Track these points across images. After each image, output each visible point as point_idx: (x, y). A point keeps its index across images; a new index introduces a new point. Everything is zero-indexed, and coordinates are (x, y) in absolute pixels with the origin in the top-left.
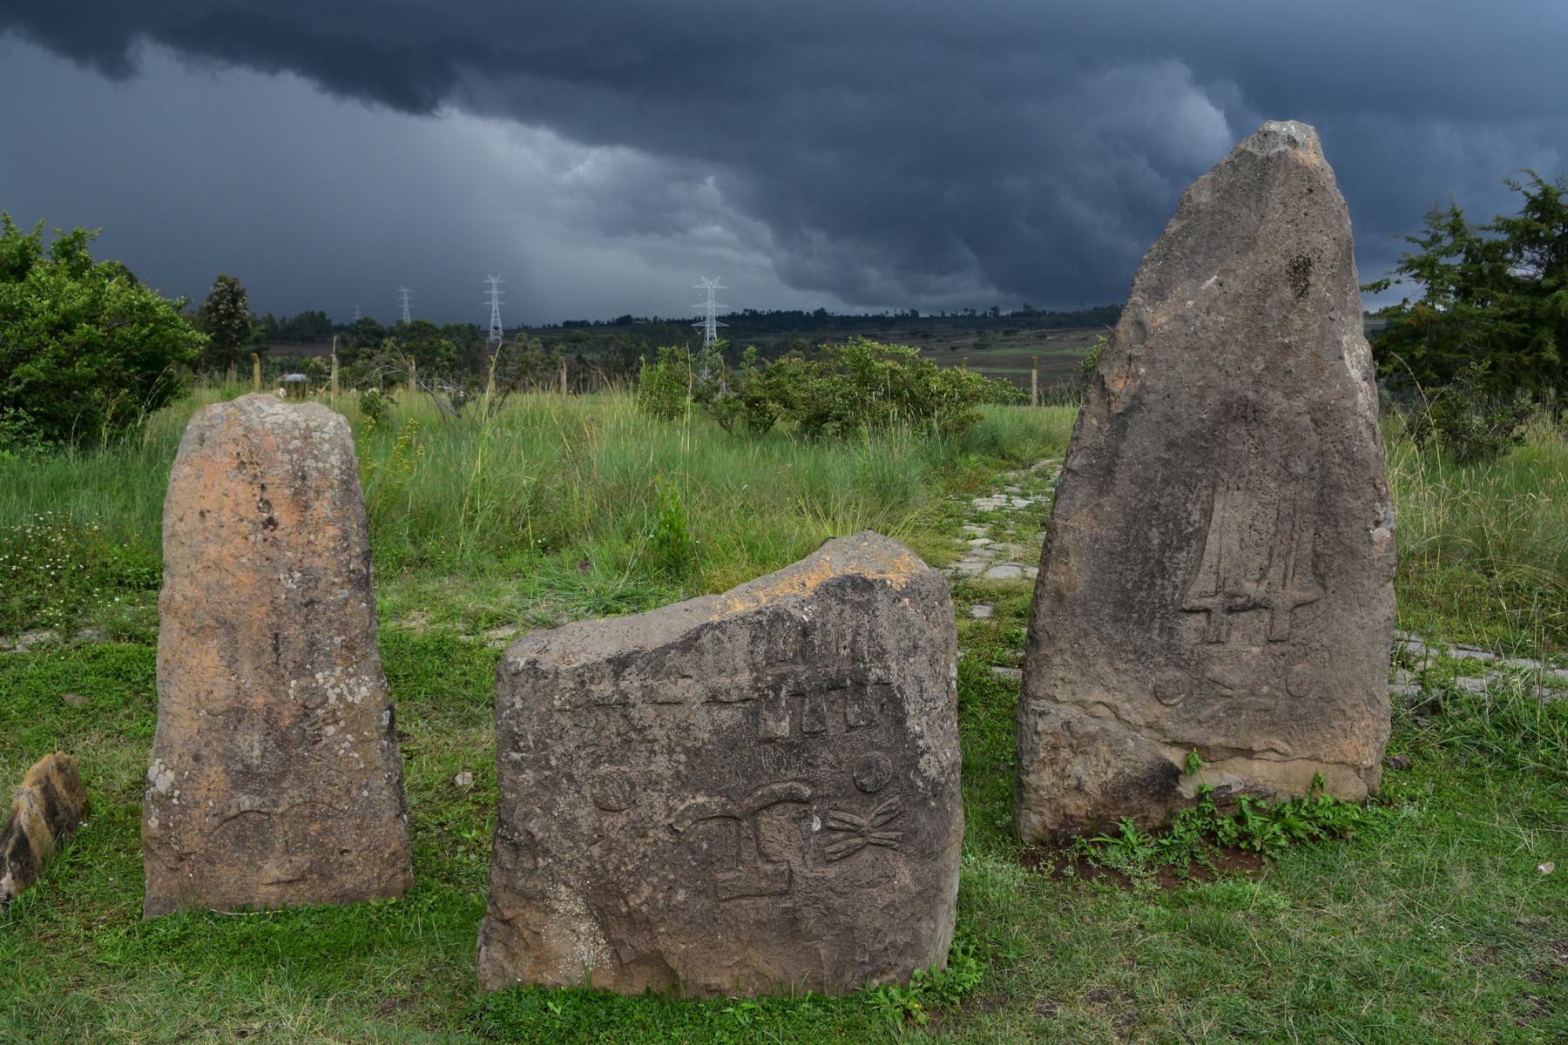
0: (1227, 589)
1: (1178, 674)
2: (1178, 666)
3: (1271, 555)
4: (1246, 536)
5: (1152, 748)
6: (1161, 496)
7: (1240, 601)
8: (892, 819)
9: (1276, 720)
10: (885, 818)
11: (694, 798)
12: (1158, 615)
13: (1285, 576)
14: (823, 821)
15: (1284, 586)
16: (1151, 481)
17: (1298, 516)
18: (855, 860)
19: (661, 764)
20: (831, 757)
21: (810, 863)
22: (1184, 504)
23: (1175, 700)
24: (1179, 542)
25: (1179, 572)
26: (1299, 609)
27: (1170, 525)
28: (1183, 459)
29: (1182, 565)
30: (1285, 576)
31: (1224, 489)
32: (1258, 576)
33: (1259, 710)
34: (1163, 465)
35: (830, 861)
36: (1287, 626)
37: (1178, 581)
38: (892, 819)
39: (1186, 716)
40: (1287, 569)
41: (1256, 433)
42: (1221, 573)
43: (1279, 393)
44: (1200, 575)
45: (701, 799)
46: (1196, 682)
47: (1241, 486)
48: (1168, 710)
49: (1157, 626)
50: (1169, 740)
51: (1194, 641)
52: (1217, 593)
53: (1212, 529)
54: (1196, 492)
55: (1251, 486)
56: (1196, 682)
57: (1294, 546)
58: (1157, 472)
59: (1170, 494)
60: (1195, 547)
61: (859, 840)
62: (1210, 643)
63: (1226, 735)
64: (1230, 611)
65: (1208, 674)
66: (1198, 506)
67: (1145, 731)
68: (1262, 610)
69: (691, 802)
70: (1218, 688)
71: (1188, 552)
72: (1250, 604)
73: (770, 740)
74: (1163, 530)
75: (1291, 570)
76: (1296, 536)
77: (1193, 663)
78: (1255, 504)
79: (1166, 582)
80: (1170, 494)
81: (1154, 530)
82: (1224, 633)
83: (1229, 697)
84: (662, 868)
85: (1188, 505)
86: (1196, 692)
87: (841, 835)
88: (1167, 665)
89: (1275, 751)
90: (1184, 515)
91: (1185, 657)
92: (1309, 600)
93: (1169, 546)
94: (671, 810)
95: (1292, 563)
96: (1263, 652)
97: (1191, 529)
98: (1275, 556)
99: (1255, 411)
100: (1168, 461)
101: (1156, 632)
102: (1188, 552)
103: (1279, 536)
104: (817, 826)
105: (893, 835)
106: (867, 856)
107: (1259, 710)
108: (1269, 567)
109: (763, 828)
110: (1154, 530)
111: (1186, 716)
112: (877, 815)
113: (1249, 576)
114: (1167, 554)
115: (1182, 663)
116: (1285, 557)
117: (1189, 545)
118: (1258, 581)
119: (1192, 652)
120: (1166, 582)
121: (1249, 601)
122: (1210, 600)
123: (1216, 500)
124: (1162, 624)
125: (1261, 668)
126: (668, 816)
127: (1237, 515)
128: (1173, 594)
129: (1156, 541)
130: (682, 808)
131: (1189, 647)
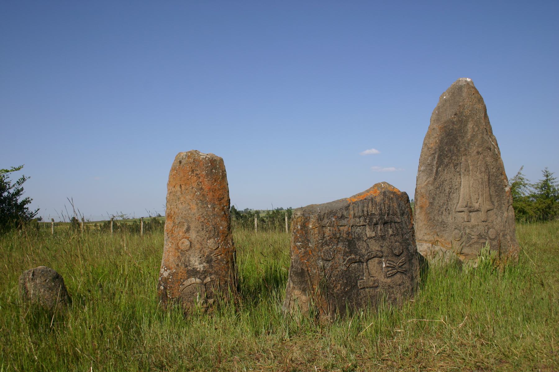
3: (479, 195)
4: (471, 189)
7: (472, 208)
8: (404, 264)
10: (402, 264)
11: (350, 256)
13: (484, 201)
14: (386, 264)
17: (484, 183)
18: (395, 277)
19: (340, 246)
20: (386, 244)
21: (383, 277)
26: (488, 212)
29: (455, 198)
30: (484, 201)
32: (476, 201)
35: (389, 277)
38: (404, 264)
40: (484, 199)
45: (353, 256)
57: (485, 192)
61: (396, 270)
64: (470, 212)
69: (350, 257)
72: (475, 210)
73: (371, 238)
75: (485, 199)
76: (485, 189)
84: (343, 279)
87: (390, 269)
91: (460, 226)
92: (491, 209)
93: (451, 192)
94: (344, 260)
95: (485, 197)
103: (480, 189)
104: (384, 266)
105: (404, 269)
106: (398, 275)
108: (479, 199)
109: (369, 266)
112: (400, 263)
116: (482, 195)
118: (477, 202)
119: (461, 225)
126: (343, 262)
130: (347, 259)
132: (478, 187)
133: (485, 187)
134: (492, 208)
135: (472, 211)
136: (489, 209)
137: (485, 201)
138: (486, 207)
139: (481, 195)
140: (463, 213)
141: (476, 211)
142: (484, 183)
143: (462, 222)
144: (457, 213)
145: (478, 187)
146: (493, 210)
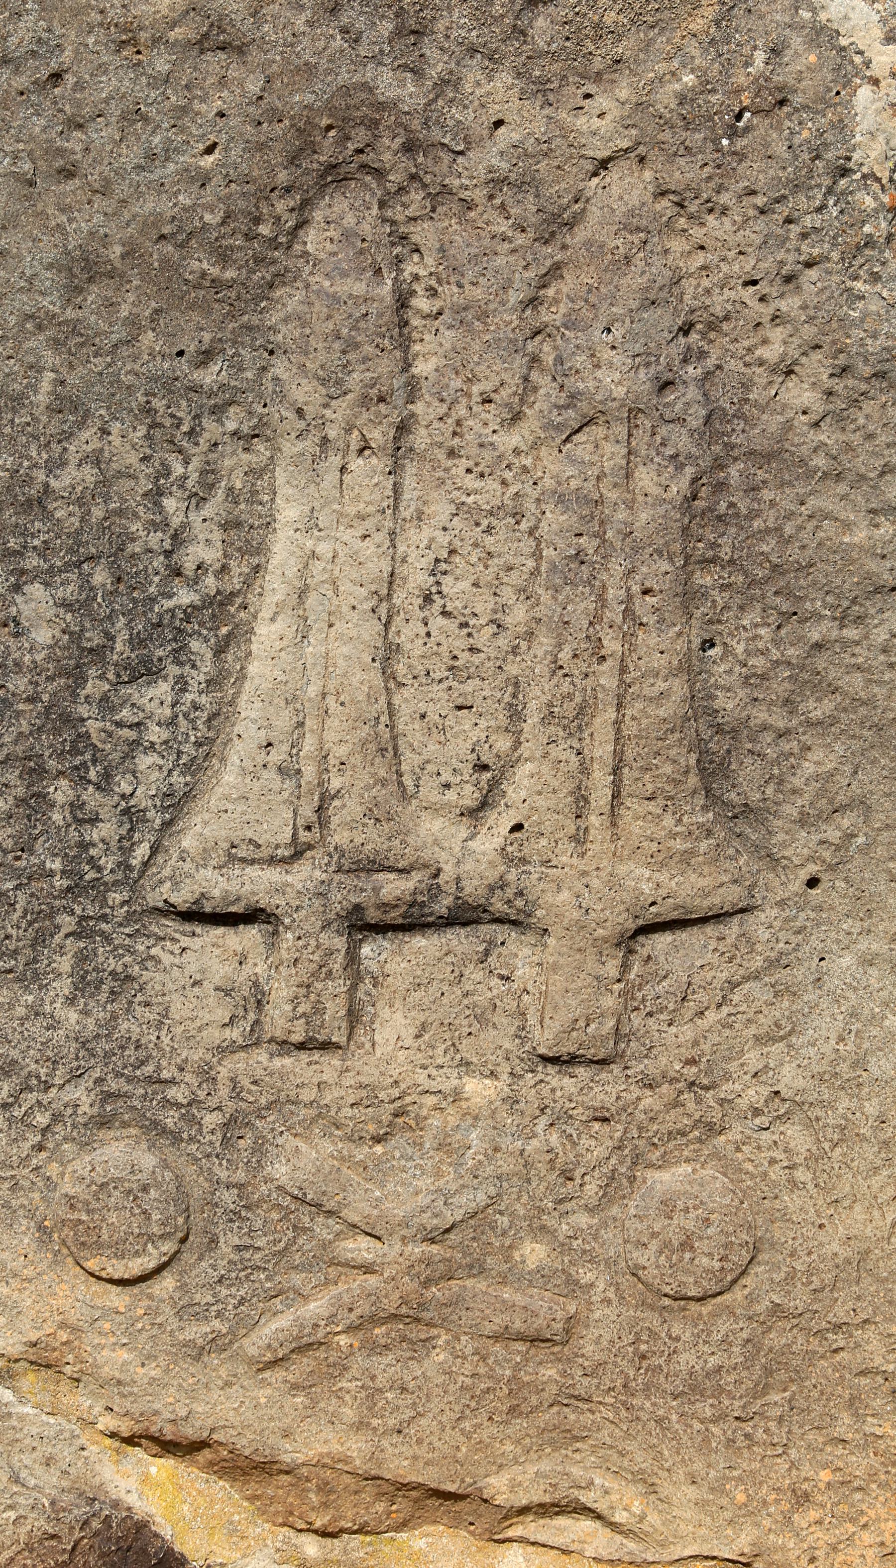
0: (340, 837)
1: (148, 1161)
2: (157, 1129)
3: (516, 714)
5: (66, 1454)
6: (56, 465)
9: (584, 1385)
12: (67, 922)
15: (579, 839)
16: (18, 401)
17: (617, 566)
22: (156, 495)
23: (136, 1266)
24: (137, 642)
25: (145, 761)
26: (662, 941)
27: (101, 577)
28: (133, 323)
29: (155, 734)
31: (309, 445)
32: (469, 796)
33: (504, 1336)
34: (56, 344)
36: (609, 1002)
37: (141, 800)
39: (196, 1332)
40: (585, 770)
41: (422, 234)
42: (309, 772)
43: (505, 78)
44: (230, 777)
46: (228, 1197)
47: (376, 436)
48: (117, 1298)
49: (65, 964)
50: (125, 1428)
51: (215, 1035)
52: (298, 852)
53: (271, 600)
54: (198, 452)
55: (420, 439)
56: (228, 1197)
58: (36, 368)
59: (96, 459)
60: (207, 667)
62: (284, 1046)
63: (360, 1426)
65: (280, 1171)
66: (208, 510)
67: (29, 1380)
68: (501, 932)
70: (324, 1229)
71: (182, 685)
72: (442, 906)
74: (70, 591)
76: (612, 645)
77: (211, 1120)
78: (441, 510)
79: (91, 797)
80: (96, 459)
81: (36, 590)
82: (335, 1009)
83: (368, 1269)
85: (170, 504)
86: (228, 1241)
88: (104, 1122)
89: (599, 1517)
90: (155, 539)
91: (177, 1094)
93: (98, 653)
96: (512, 1101)
97: (185, 597)
98: (533, 719)
99: (409, 148)
100: (74, 328)
101: (64, 986)
102: (182, 685)
103: (544, 642)
107: (504, 1336)
108: (510, 763)
110: (36, 590)
111: (196, 1332)
113: (430, 792)
114: (93, 687)
115: (170, 1118)
117: (180, 655)
119: (207, 1075)
120: (91, 797)
121: (435, 891)
122: (274, 875)
123: (284, 491)
124: (82, 958)
125: (506, 1165)
127: (368, 548)
128: (126, 845)
129: (43, 635)
131: (196, 1056)
132: (518, 615)
133: (614, 613)
134: (732, 895)
135: (394, 917)
136: (665, 911)
137: (601, 797)
138: (614, 883)
139: (549, 717)
140: (251, 934)
141: (450, 921)
142: (617, 566)
143: (225, 1050)
144: (171, 925)
145: (518, 615)
146: (732, 929)
